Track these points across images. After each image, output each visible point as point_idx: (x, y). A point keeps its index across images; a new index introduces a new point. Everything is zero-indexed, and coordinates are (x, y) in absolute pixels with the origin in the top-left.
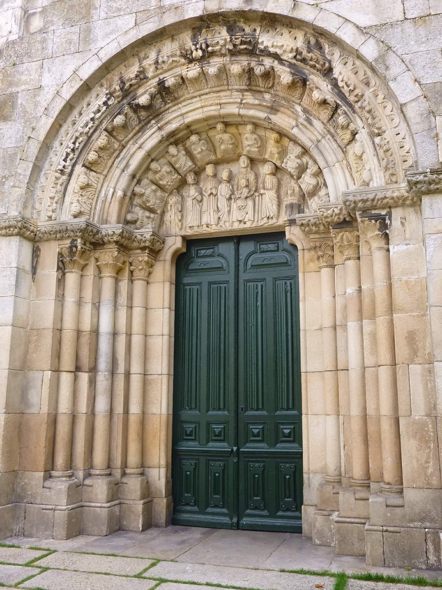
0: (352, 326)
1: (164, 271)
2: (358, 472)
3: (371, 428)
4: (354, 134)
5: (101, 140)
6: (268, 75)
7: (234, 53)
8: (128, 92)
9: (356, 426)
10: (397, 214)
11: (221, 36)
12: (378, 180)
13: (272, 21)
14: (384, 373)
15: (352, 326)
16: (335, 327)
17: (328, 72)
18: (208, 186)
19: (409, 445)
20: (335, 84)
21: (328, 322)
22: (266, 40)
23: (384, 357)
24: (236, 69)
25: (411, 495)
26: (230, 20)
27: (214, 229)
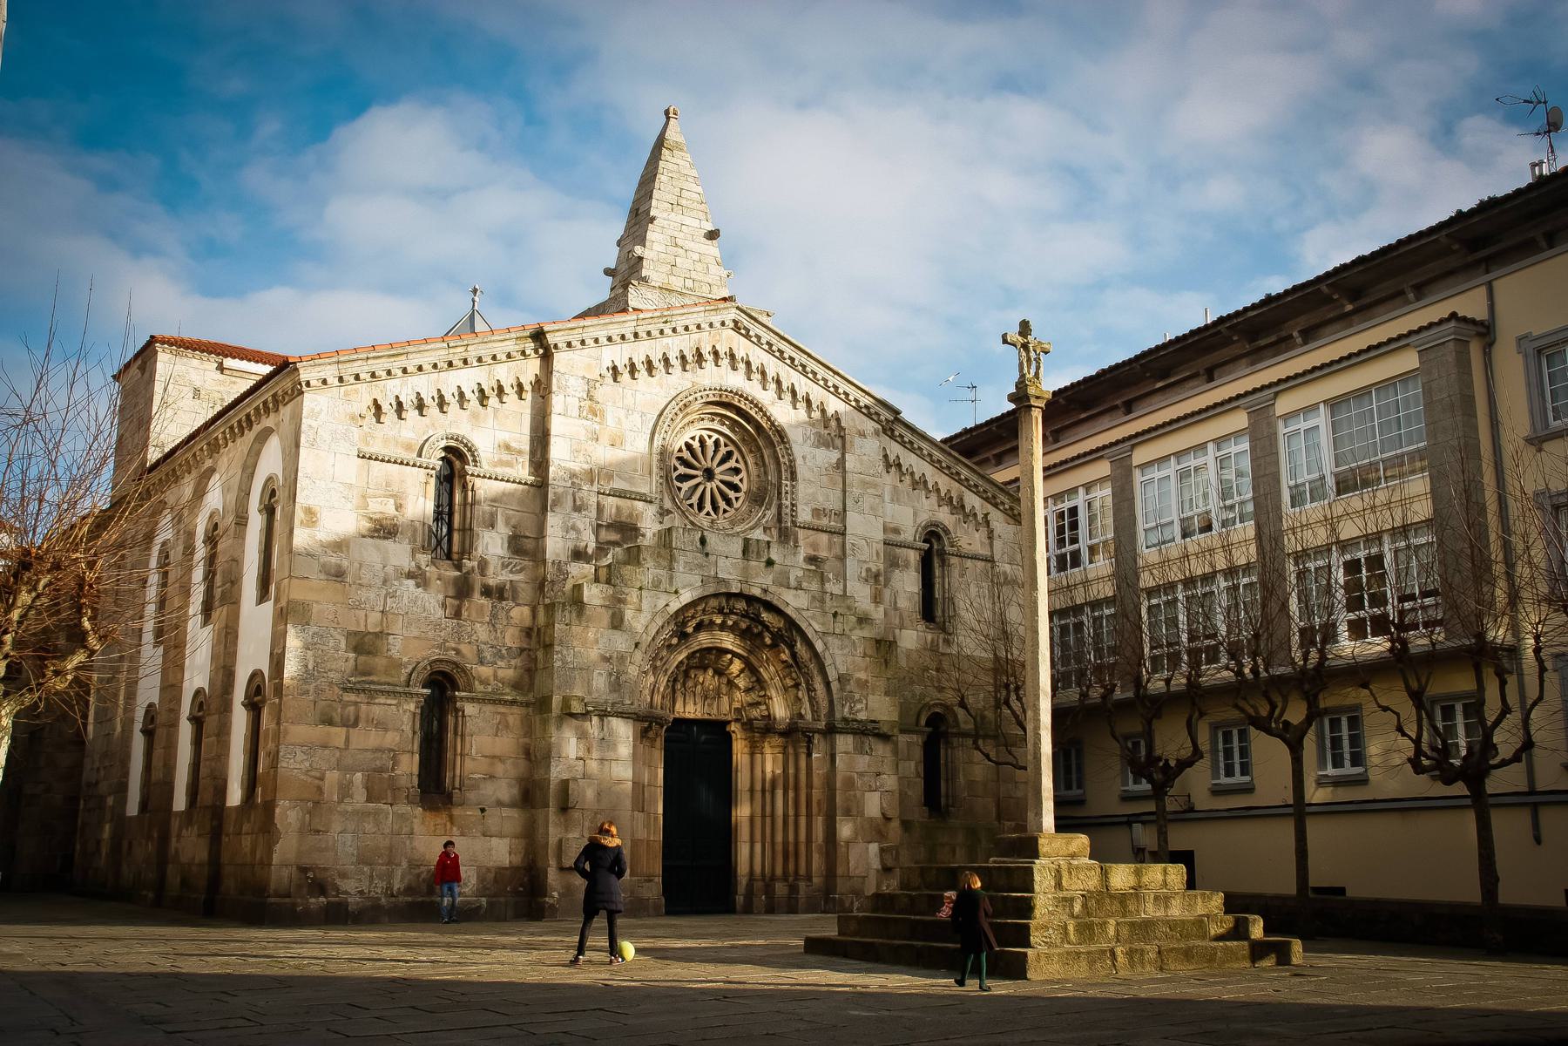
0: (779, 793)
1: (660, 743)
2: (779, 871)
3: (791, 848)
4: (797, 686)
5: (664, 653)
6: (760, 635)
7: (745, 615)
8: (684, 624)
9: (779, 848)
10: (816, 736)
11: (741, 605)
12: (809, 717)
13: (771, 607)
14: (803, 821)
15: (779, 793)
16: (763, 791)
17: (791, 647)
18: (690, 684)
19: (816, 857)
20: (794, 655)
21: (758, 787)
22: (765, 616)
23: (803, 810)
24: (743, 626)
25: (815, 880)
26: (750, 599)
27: (692, 716)
